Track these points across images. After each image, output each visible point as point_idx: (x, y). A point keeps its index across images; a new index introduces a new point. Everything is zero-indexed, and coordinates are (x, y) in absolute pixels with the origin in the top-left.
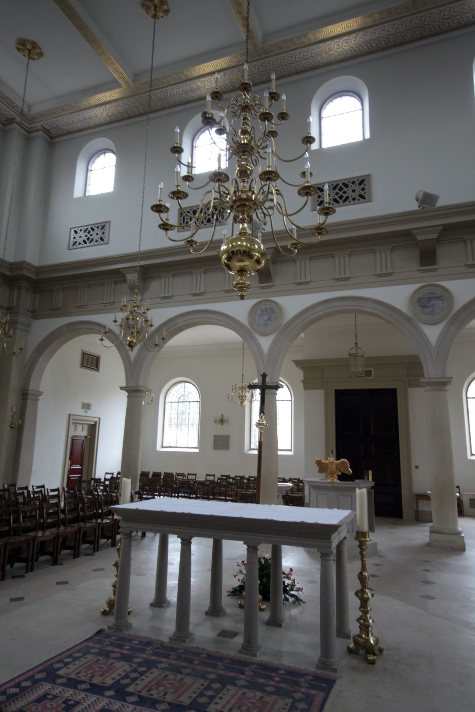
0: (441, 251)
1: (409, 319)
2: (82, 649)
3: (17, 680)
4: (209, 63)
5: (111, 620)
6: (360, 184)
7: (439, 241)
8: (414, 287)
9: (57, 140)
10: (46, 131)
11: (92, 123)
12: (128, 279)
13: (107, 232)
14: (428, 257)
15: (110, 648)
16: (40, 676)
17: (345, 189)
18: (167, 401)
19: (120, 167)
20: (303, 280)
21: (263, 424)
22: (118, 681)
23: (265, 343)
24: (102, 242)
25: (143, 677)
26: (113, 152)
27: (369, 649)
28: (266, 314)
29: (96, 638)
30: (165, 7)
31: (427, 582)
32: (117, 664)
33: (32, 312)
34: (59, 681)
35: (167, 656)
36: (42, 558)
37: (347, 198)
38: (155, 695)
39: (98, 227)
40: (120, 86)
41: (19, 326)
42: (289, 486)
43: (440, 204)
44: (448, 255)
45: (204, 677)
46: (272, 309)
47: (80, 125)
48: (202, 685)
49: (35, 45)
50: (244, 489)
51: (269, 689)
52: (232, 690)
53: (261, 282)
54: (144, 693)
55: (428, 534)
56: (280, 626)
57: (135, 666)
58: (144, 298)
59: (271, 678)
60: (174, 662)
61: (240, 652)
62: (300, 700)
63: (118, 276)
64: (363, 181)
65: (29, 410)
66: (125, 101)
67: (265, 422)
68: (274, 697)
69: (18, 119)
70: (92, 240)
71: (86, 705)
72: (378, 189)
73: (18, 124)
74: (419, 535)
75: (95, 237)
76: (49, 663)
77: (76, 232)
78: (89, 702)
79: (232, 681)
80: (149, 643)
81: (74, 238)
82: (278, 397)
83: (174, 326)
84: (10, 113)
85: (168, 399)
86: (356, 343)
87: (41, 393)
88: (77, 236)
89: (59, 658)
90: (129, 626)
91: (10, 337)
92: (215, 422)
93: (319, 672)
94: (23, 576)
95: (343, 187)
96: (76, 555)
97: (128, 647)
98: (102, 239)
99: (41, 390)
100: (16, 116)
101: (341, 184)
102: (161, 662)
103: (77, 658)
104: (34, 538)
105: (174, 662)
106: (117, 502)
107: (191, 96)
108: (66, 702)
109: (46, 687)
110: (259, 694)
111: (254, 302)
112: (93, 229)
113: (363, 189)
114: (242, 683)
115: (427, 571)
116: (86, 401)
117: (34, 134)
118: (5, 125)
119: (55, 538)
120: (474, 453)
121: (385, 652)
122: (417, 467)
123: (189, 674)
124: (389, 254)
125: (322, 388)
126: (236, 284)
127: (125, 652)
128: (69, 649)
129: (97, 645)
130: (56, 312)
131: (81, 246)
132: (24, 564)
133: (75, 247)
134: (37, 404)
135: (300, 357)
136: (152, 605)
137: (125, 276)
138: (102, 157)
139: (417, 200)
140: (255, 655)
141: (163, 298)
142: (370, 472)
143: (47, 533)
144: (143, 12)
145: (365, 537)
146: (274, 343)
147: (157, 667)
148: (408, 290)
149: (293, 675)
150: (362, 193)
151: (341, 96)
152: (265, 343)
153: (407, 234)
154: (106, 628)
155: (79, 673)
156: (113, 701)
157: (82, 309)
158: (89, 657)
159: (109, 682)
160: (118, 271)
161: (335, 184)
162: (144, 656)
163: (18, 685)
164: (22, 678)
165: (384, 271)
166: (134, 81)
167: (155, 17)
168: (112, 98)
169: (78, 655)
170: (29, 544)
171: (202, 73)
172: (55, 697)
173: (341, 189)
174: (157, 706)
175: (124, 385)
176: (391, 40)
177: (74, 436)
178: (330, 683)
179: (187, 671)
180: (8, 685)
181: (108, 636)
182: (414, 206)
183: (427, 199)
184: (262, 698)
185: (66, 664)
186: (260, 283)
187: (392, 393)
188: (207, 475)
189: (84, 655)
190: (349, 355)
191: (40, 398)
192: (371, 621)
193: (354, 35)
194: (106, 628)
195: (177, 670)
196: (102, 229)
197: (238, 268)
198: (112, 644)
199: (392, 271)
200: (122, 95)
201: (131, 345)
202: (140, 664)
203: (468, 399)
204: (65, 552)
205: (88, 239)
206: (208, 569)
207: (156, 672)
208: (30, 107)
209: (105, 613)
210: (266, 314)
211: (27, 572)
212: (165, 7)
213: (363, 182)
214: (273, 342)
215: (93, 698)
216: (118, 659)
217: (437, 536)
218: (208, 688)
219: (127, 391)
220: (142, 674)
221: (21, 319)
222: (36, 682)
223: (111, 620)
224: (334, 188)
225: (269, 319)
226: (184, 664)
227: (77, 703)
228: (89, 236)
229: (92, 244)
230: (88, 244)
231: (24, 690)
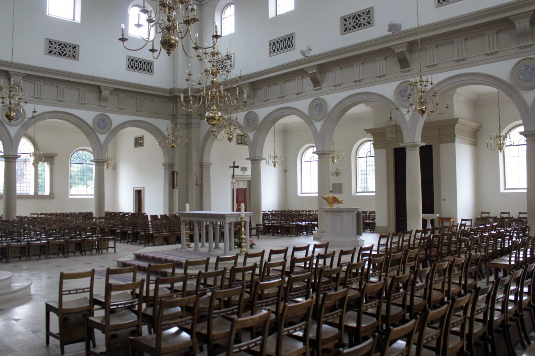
6: (367, 14)
18: (303, 161)
19: (238, 14)
23: (318, 125)
28: (318, 106)
41: (193, 125)
43: (403, 29)
46: (321, 104)
64: (369, 11)
65: (205, 175)
83: (272, 119)
86: (391, 118)
111: (312, 99)
122: (444, 200)
125: (384, 148)
134: (209, 171)
135: (372, 127)
138: (229, 7)
148: (395, 85)
152: (318, 125)
153: (388, 49)
175: (249, 157)
177: (237, 189)
191: (211, 167)
210: (318, 106)
213: (369, 12)
214: (322, 125)
219: (251, 160)
221: (194, 121)
225: (320, 111)
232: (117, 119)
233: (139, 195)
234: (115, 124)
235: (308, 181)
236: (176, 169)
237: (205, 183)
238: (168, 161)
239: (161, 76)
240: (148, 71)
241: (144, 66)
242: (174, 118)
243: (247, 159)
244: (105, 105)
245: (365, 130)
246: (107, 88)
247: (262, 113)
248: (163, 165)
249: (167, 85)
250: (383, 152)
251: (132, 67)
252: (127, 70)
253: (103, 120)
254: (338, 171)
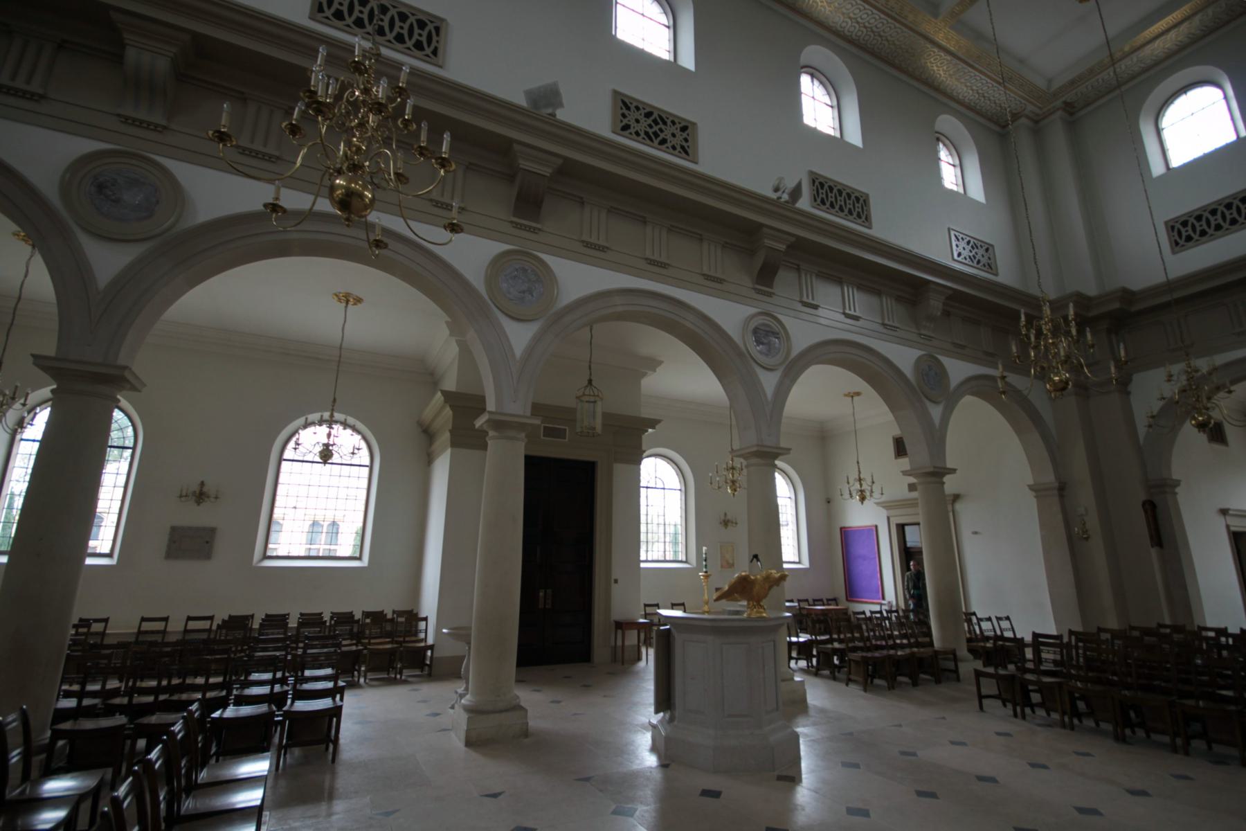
8: (752, 311)
86: (590, 381)
146: (537, 339)
254: (205, 489)
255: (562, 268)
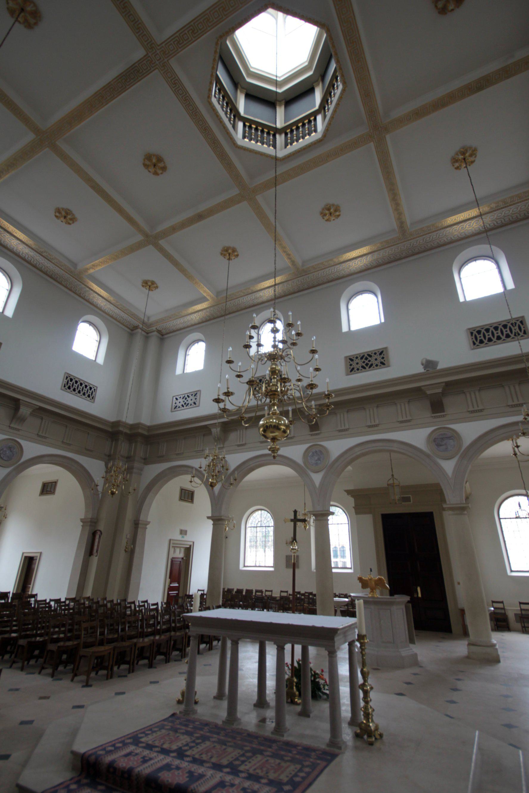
0: (447, 401)
1: (428, 456)
2: (160, 726)
3: (113, 743)
4: (267, 281)
5: (182, 707)
7: (444, 393)
8: (430, 430)
9: (166, 336)
10: (159, 331)
11: (189, 324)
12: (213, 432)
13: (198, 398)
14: (437, 406)
15: (179, 726)
16: (129, 741)
17: (369, 359)
18: (247, 526)
20: (343, 428)
21: (295, 549)
22: (180, 748)
23: (317, 478)
24: (195, 405)
25: (199, 746)
26: (203, 341)
27: (370, 734)
28: (316, 455)
29: (170, 719)
30: (236, 253)
31: (455, 690)
32: (182, 737)
33: (145, 459)
34: (141, 745)
35: (218, 734)
36: (141, 662)
37: (372, 365)
38: (204, 757)
39: (192, 395)
40: (207, 300)
41: (135, 470)
42: (346, 601)
44: (453, 404)
45: (242, 749)
46: (321, 451)
47: (181, 326)
48: (239, 753)
49: (153, 283)
50: (305, 603)
51: (286, 758)
52: (259, 757)
53: (311, 431)
54: (197, 756)
55: (466, 647)
56: (308, 716)
57: (194, 738)
58: (225, 446)
59: (290, 751)
60: (222, 738)
61: (272, 733)
62: (307, 766)
63: (205, 431)
65: (139, 537)
66: (211, 309)
67: (297, 548)
68: (288, 763)
69: (141, 326)
70: (188, 404)
71: (156, 760)
72: (393, 357)
73: (141, 329)
74: (459, 648)
75: (190, 402)
76: (135, 733)
77: (177, 399)
78: (159, 759)
79: (261, 752)
80: (207, 724)
81: (176, 403)
82: (329, 522)
84: (136, 323)
85: (249, 525)
86: (393, 475)
87: (149, 523)
88: (177, 402)
89: (143, 731)
90: (195, 712)
91: (127, 480)
92: (287, 543)
93: (328, 749)
94: (126, 676)
95: (368, 357)
96: (167, 661)
97: (191, 726)
98: (195, 403)
99: (148, 520)
100: (140, 324)
101: (366, 355)
102: (212, 737)
103: (155, 732)
104: (135, 644)
105: (222, 738)
106: (191, 611)
107: (256, 302)
108: (144, 757)
109: (132, 748)
110: (278, 761)
111: (308, 445)
112: (188, 396)
113: (383, 358)
114: (268, 753)
115: (459, 680)
116: (183, 528)
117: (150, 334)
118: (132, 330)
119: (151, 644)
120: (513, 569)
121: (384, 737)
123: (231, 746)
124: (407, 405)
125: (370, 513)
126: (270, 448)
127: (189, 729)
128: (150, 725)
129: (170, 724)
130: (161, 459)
131: (180, 409)
132: (127, 666)
133: (176, 410)
134: (145, 531)
135: (351, 487)
136: (215, 698)
137: (210, 430)
138: (196, 345)
139: (422, 364)
140: (283, 736)
141: (239, 446)
142: (419, 589)
143: (146, 640)
144: (222, 258)
145: (364, 639)
147: (209, 740)
149: (308, 750)
150: (382, 360)
151: (362, 294)
152: (317, 478)
153: (418, 390)
154: (178, 712)
155: (155, 741)
156: (174, 759)
157: (180, 456)
158: (163, 731)
159: (174, 747)
160: (206, 427)
161: (362, 355)
162: (202, 732)
163: (114, 745)
164: (117, 741)
165: (405, 419)
166: (217, 296)
167: (229, 259)
168: (202, 308)
169: (156, 729)
170: (131, 648)
171: (262, 287)
172: (137, 754)
173: (366, 359)
174: (204, 764)
175: (210, 515)
176: (392, 257)
177: (173, 558)
178: (334, 756)
179: (230, 744)
180: (107, 745)
181: (178, 718)
182: (421, 369)
183: (429, 364)
184: (279, 764)
185: (147, 735)
186: (311, 431)
187: (430, 515)
188: (281, 592)
189: (160, 730)
190: (388, 485)
191: (148, 526)
192: (370, 710)
193: (365, 257)
194: (178, 712)
195: (223, 743)
196: (195, 396)
197: (271, 437)
198: (180, 724)
199: (410, 418)
200: (209, 305)
201: (212, 485)
202: (198, 738)
203: (501, 520)
204: (159, 657)
205: (185, 404)
206: (273, 675)
207: (208, 743)
208: (149, 318)
209: (179, 702)
211: (129, 673)
212: (236, 253)
214: (322, 478)
215: (162, 757)
216: (183, 734)
217: (474, 648)
218: (243, 755)
219: (213, 520)
220: (198, 744)
221: (136, 465)
222: (125, 744)
223: (182, 707)
224: (362, 358)
225: (319, 459)
226: (230, 740)
227: (151, 759)
228: (186, 401)
229: (187, 407)
230: (185, 407)
231: (117, 749)
232: (31, 449)
233: (29, 566)
234: (27, 456)
235: (258, 551)
236: (101, 527)
237: (137, 549)
238: (90, 516)
239: (101, 407)
240: (89, 396)
241: (85, 390)
242: (109, 458)
243: (208, 518)
244: (20, 428)
245: (346, 491)
246: (28, 405)
247: (234, 460)
248: (82, 520)
249: (112, 418)
250: (368, 519)
251: (69, 388)
252: (61, 389)
253: (10, 448)
255: (328, 444)
